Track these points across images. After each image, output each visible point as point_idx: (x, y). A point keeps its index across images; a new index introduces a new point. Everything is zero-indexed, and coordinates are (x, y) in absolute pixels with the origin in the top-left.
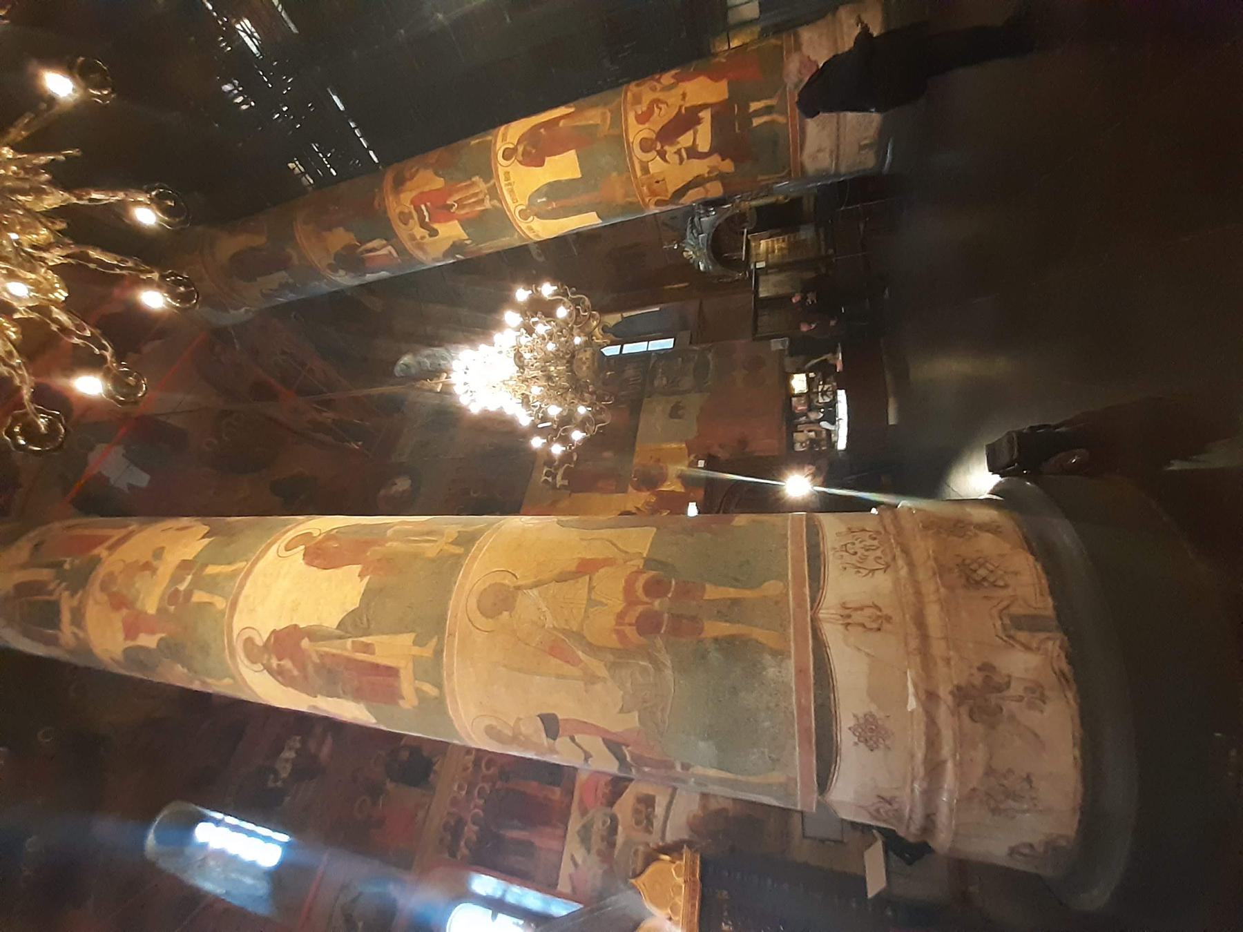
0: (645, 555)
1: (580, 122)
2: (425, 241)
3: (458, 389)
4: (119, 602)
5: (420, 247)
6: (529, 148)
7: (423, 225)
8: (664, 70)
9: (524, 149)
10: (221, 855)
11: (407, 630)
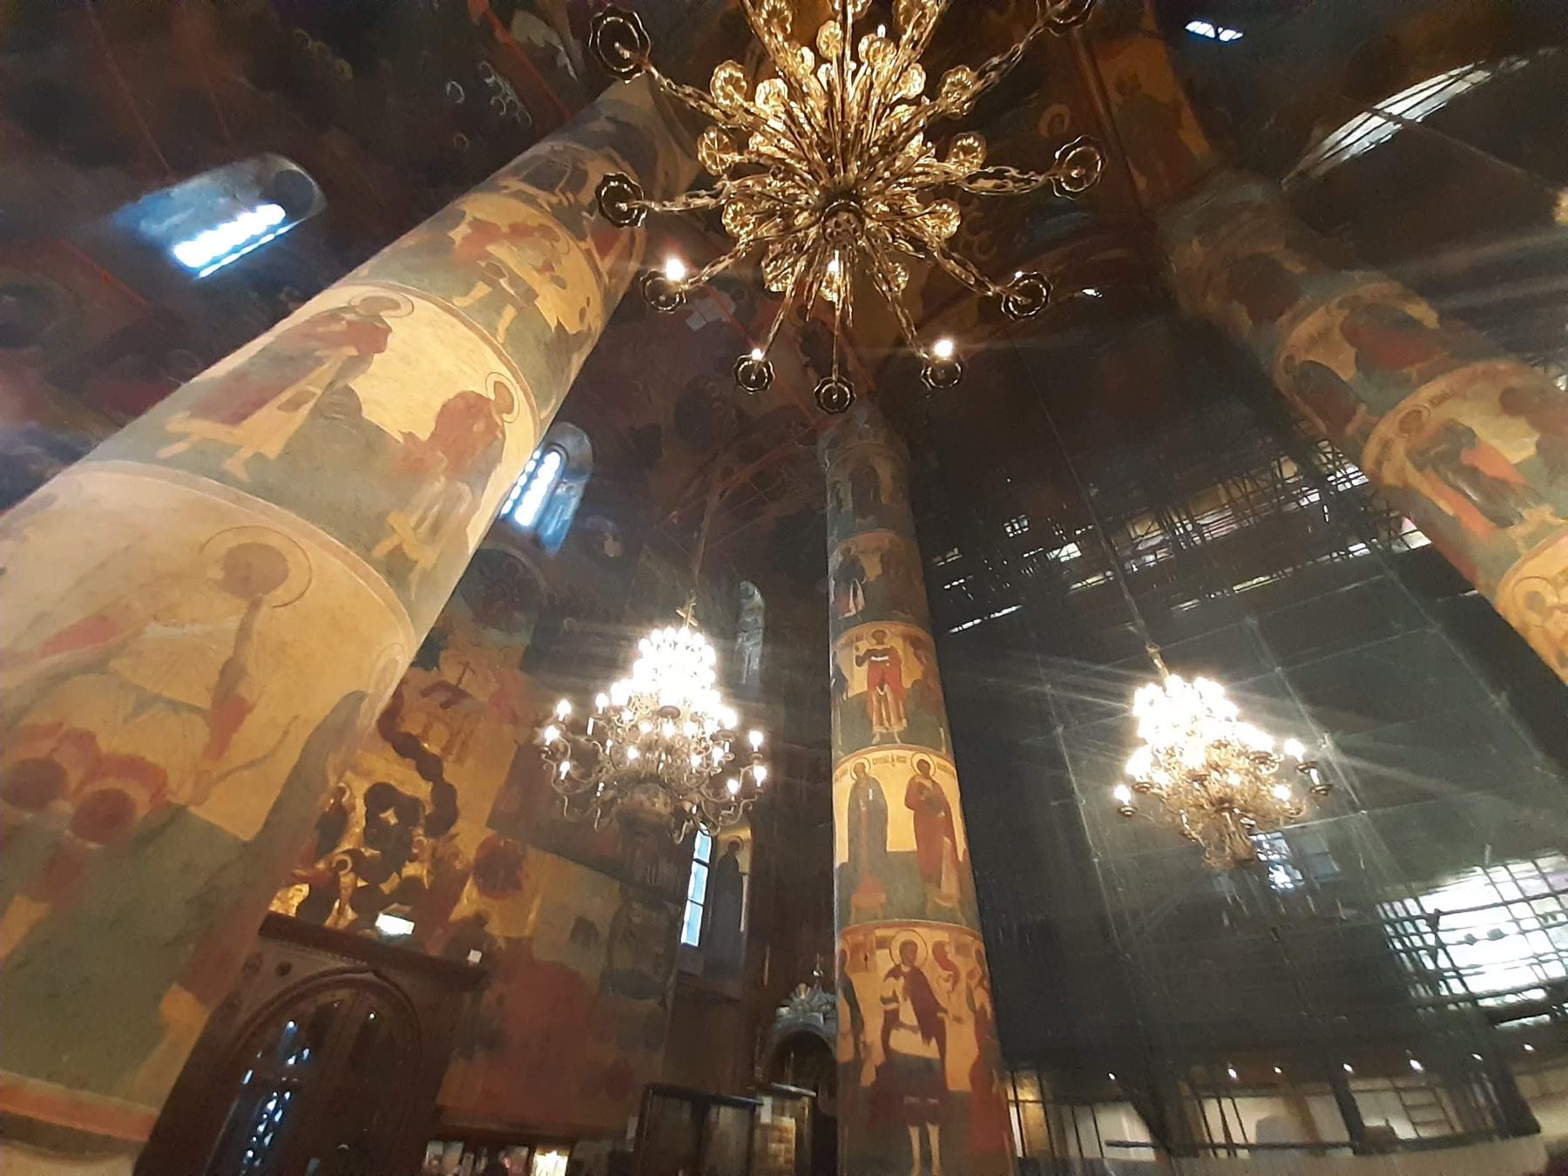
0: (192, 809)
1: (946, 866)
2: (854, 650)
3: (669, 632)
4: (518, 232)
5: (849, 644)
6: (926, 793)
7: (870, 653)
8: (994, 995)
9: (929, 789)
10: (229, 216)
11: (289, 451)
